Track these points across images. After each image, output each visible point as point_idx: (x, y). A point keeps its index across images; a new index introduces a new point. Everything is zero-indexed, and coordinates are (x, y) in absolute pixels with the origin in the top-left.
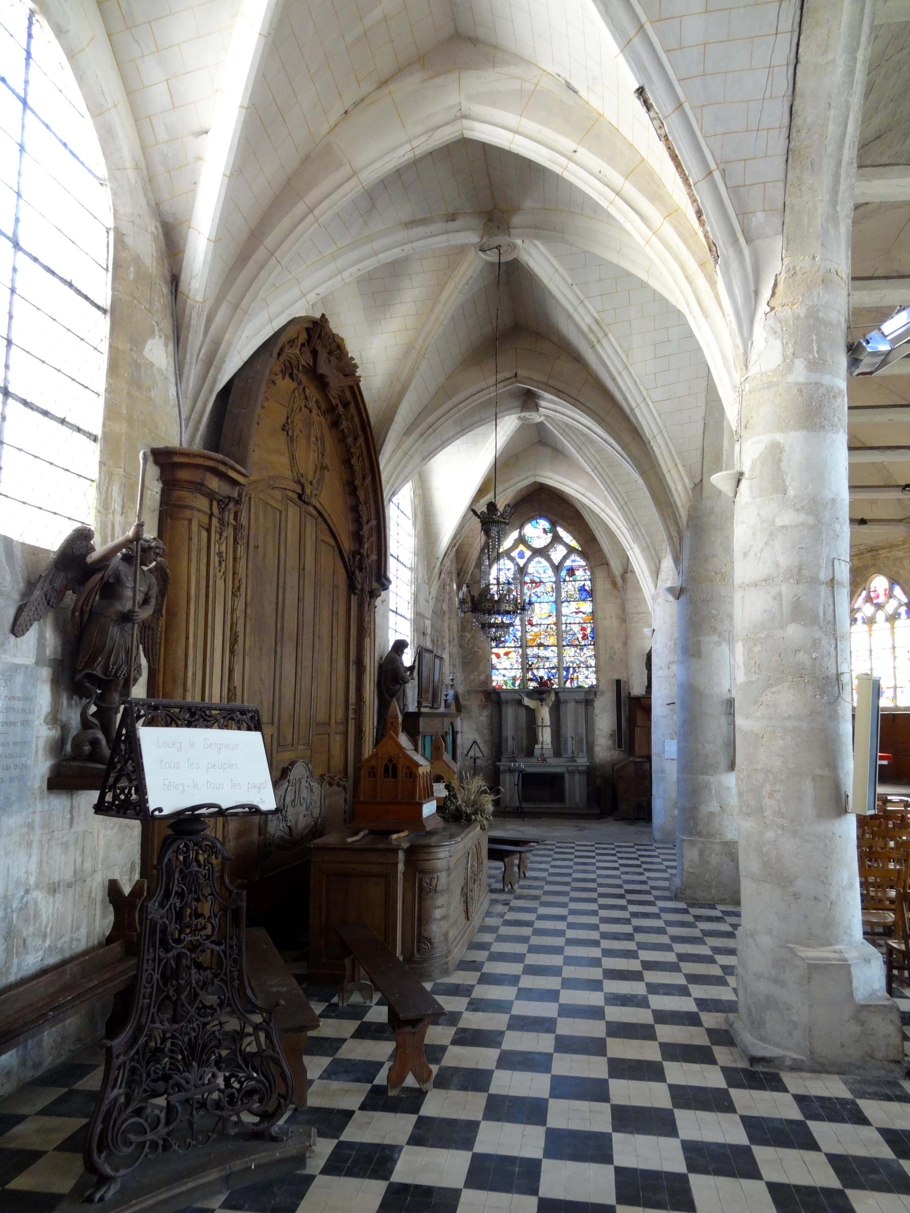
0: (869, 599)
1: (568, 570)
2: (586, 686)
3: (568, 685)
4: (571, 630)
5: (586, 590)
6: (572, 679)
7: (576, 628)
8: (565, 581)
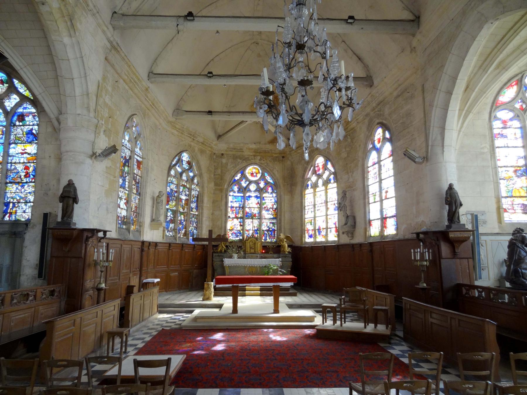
0: (315, 172)
1: (19, 116)
2: (23, 220)
3: (7, 218)
4: (15, 168)
5: (33, 134)
6: (11, 214)
7: (20, 167)
8: (15, 125)
